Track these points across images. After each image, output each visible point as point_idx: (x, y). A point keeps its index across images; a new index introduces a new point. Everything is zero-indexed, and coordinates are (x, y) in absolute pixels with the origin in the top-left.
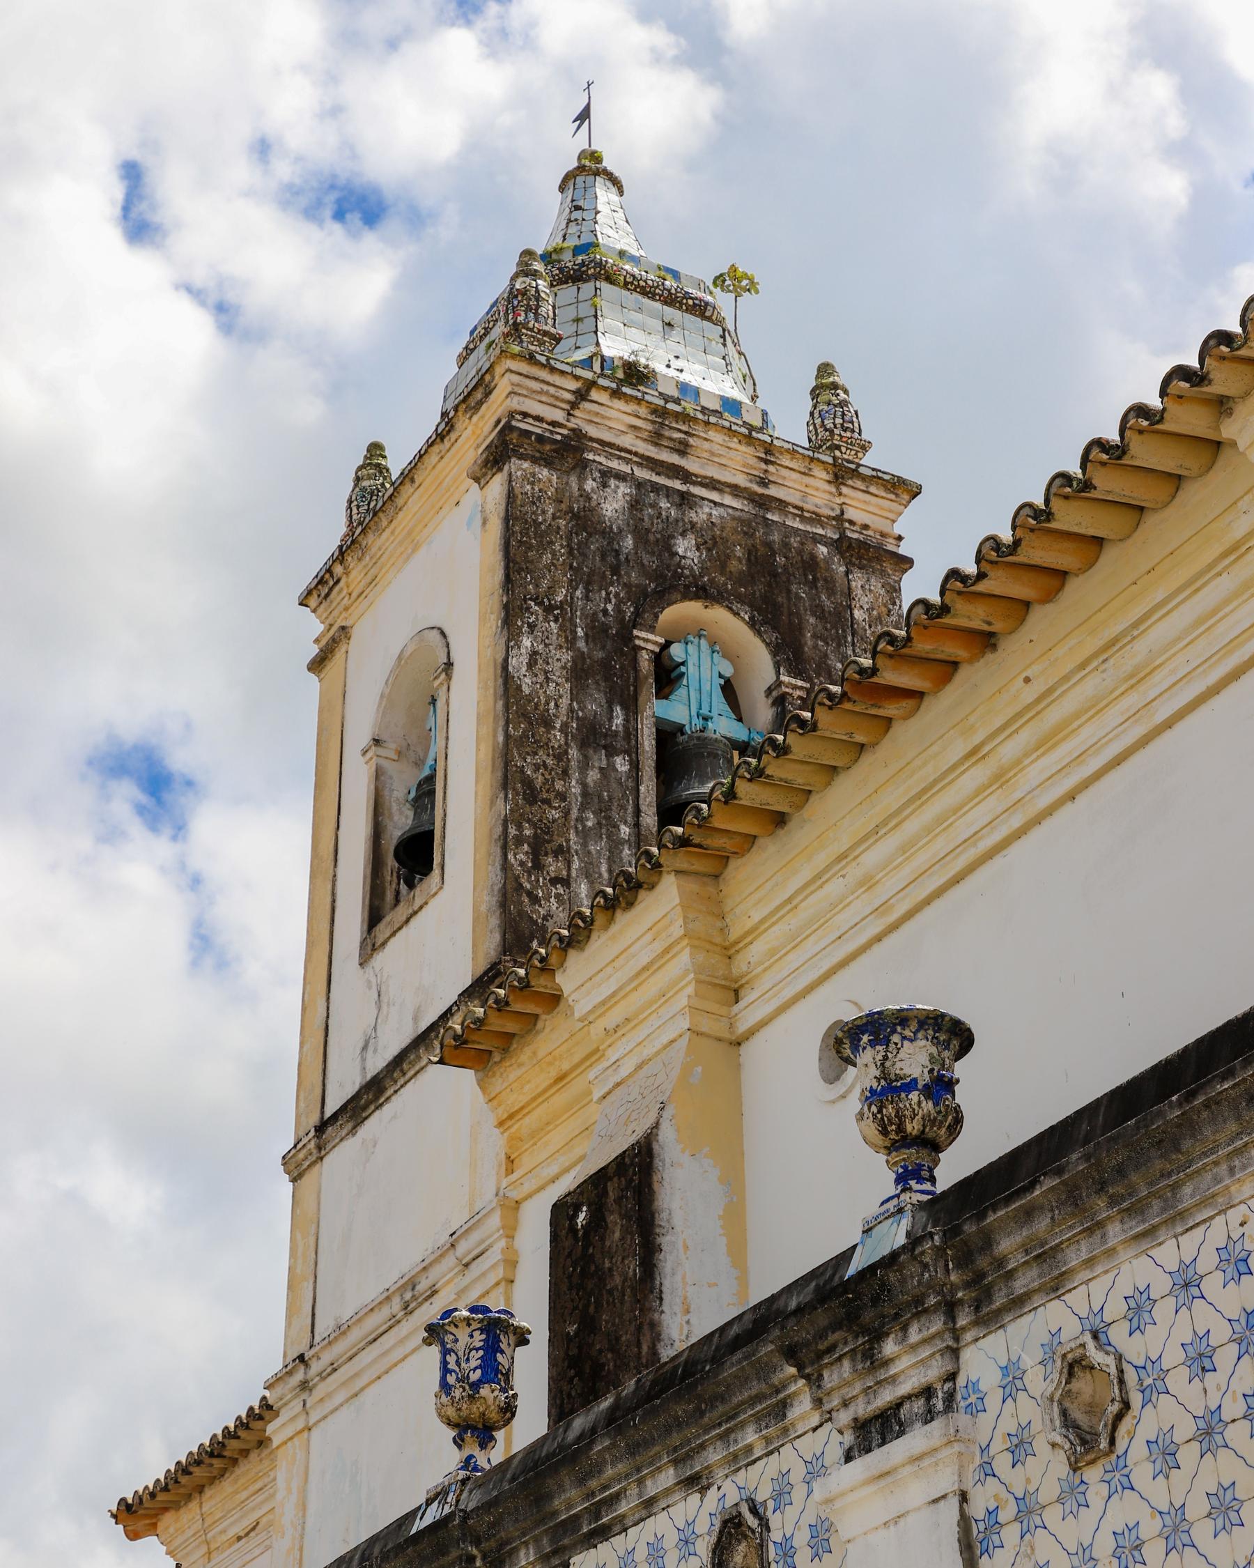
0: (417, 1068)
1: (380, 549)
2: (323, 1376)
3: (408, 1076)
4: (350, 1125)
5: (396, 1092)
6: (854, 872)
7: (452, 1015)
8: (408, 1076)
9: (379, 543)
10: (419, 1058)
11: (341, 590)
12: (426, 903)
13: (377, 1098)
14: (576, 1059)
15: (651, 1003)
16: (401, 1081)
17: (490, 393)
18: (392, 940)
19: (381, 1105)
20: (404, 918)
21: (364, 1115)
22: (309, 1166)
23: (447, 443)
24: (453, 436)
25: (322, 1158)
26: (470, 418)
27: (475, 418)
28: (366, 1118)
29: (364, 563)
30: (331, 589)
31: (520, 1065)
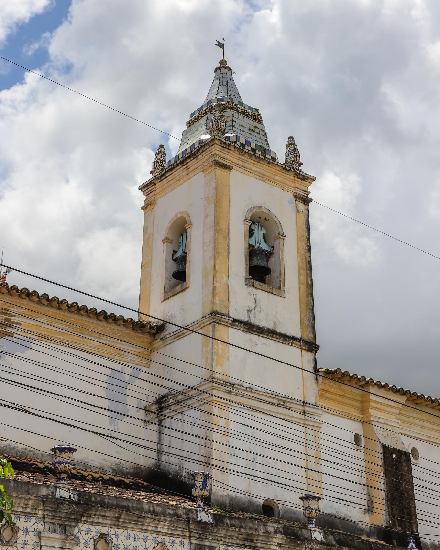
0: (278, 340)
1: (247, 161)
2: (236, 395)
3: (273, 338)
4: (245, 330)
6: (422, 423)
7: (296, 341)
8: (273, 338)
9: (248, 159)
10: (280, 339)
11: (229, 152)
13: (259, 333)
14: (350, 396)
15: (386, 411)
16: (269, 337)
17: (304, 180)
18: (260, 291)
19: (259, 336)
20: (269, 291)
23: (284, 171)
24: (287, 172)
25: (229, 326)
26: (294, 177)
27: (296, 179)
29: (240, 157)
30: (226, 148)
31: (335, 384)
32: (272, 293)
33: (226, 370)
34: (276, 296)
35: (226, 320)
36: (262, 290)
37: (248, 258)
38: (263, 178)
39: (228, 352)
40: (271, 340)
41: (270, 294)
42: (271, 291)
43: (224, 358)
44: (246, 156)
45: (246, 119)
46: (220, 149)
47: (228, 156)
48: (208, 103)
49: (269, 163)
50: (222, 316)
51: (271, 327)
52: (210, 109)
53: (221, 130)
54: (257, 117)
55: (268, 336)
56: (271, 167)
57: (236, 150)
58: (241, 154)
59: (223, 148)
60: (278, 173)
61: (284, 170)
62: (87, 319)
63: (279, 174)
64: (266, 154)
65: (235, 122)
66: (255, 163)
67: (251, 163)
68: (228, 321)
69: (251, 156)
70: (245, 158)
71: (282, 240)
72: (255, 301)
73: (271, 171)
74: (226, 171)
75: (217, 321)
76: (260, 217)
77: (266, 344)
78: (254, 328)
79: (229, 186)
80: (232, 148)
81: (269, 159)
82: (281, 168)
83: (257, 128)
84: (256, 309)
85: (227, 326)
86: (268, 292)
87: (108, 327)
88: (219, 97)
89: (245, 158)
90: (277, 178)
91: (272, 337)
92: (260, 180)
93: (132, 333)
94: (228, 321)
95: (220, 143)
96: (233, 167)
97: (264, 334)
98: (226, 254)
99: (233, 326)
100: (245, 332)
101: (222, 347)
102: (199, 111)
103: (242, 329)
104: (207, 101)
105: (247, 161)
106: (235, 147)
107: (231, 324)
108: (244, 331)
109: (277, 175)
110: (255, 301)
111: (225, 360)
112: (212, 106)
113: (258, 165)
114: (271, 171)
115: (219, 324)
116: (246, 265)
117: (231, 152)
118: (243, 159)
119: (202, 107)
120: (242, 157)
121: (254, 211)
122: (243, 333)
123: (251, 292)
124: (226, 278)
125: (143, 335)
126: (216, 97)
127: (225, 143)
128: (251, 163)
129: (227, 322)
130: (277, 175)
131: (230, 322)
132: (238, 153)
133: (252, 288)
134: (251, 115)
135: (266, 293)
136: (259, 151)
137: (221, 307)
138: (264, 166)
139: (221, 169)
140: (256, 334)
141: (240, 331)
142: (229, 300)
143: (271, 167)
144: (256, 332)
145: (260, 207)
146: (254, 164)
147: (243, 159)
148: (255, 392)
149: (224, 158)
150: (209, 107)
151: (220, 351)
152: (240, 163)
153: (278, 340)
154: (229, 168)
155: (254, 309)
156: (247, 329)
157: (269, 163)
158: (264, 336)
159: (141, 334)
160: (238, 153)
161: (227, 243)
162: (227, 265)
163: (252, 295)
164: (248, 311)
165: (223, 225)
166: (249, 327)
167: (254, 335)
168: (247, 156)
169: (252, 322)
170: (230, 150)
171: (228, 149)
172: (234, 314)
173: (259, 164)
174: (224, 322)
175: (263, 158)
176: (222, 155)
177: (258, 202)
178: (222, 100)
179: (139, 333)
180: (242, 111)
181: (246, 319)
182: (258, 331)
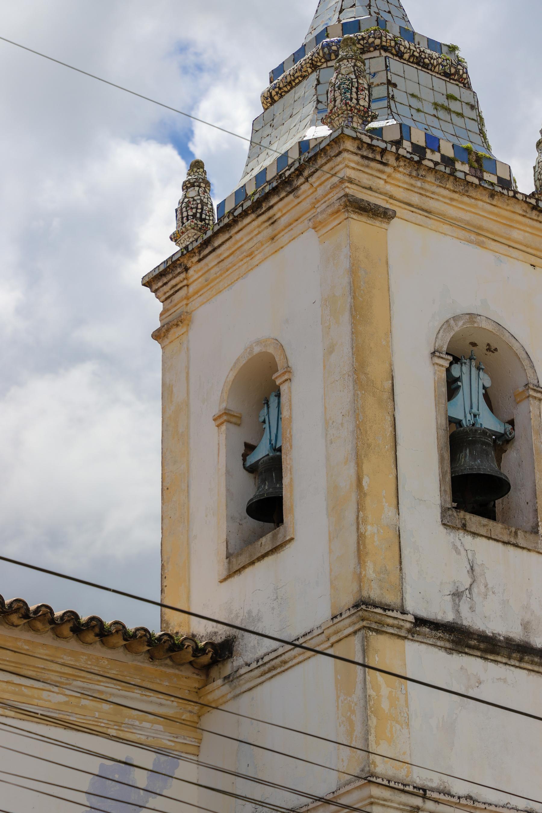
0: (536, 668)
1: (433, 193)
3: (522, 665)
4: (448, 645)
5: (506, 664)
9: (434, 189)
11: (383, 172)
12: (529, 550)
13: (485, 651)
16: (513, 662)
18: (484, 540)
19: (486, 659)
20: (506, 539)
21: (467, 650)
22: (392, 634)
23: (534, 214)
25: (405, 638)
28: (466, 653)
29: (413, 181)
30: (373, 160)
32: (516, 546)
33: (404, 753)
34: (525, 552)
35: (396, 622)
36: (489, 538)
37: (447, 456)
38: (477, 234)
39: (407, 707)
40: (518, 670)
41: (511, 549)
42: (513, 540)
43: (397, 722)
44: (430, 178)
45: (424, 77)
46: (358, 164)
47: (382, 182)
48: (318, 38)
49: (492, 196)
50: (385, 610)
51: (516, 633)
52: (324, 53)
53: (359, 110)
54: (453, 70)
55: (510, 658)
56: (499, 204)
57: (402, 163)
58: (414, 173)
59: (366, 162)
60: (518, 222)
61: (534, 212)
62: (28, 636)
63: (518, 222)
64: (482, 171)
65: (395, 85)
66: (456, 196)
67: (444, 197)
68: (402, 623)
69: (442, 178)
70: (427, 186)
71: (537, 402)
72: (472, 568)
73: (498, 215)
74: (378, 223)
75: (374, 626)
76: (474, 344)
77: (505, 681)
78: (471, 639)
79: (387, 263)
80: (391, 160)
81: (492, 184)
82: (525, 206)
83: (456, 99)
84: (475, 590)
85: (399, 636)
86: (504, 543)
87: (83, 654)
88: (348, 17)
89: (427, 186)
90: (516, 234)
91: (521, 660)
92: (471, 242)
93: (148, 666)
94: (402, 623)
95: (359, 148)
96: (394, 212)
97: (498, 654)
98: (389, 446)
99: (416, 637)
100: (449, 651)
101: (391, 692)
102: (295, 61)
103: (439, 643)
104: (315, 33)
105: (433, 193)
106: (398, 158)
107: (409, 631)
108: (446, 649)
109: (515, 225)
110: (472, 568)
111: (398, 727)
112: (328, 45)
113: (462, 202)
114: (498, 215)
115: (377, 631)
116: (443, 474)
117: (388, 170)
118: (421, 188)
119: (302, 51)
120: (419, 184)
121: (456, 329)
122: (442, 654)
123: (458, 544)
124: (389, 512)
125: (177, 672)
126: (339, 21)
127: (371, 147)
128: (444, 197)
129: (400, 628)
130: (517, 226)
131: (408, 625)
132: (407, 171)
133: (461, 533)
134: (438, 64)
135: (500, 545)
136: (463, 163)
137: (381, 588)
138: (480, 203)
139: (364, 219)
140: (479, 654)
141: (436, 650)
142: (401, 569)
143: (499, 204)
144: (478, 649)
145: (472, 316)
146: (452, 199)
147: (421, 188)
148: (483, 806)
149: (370, 189)
150: (323, 48)
151: (385, 705)
152: (415, 199)
153: (536, 668)
154: (384, 215)
155: (470, 589)
156: (453, 642)
157: (492, 196)
158: (499, 658)
159: (172, 667)
160: (407, 171)
161: (389, 419)
162: (392, 477)
163: (463, 553)
164: (454, 594)
165: (376, 369)
166: (459, 638)
167: (472, 659)
168: (433, 181)
169: (465, 623)
170: (385, 164)
171: (382, 163)
172: (417, 605)
173: (466, 199)
174: (392, 626)
175: (476, 181)
176: (365, 180)
177: (467, 303)
178: (356, 26)
179: (166, 665)
180: (413, 55)
181: (449, 617)
182: (482, 646)
